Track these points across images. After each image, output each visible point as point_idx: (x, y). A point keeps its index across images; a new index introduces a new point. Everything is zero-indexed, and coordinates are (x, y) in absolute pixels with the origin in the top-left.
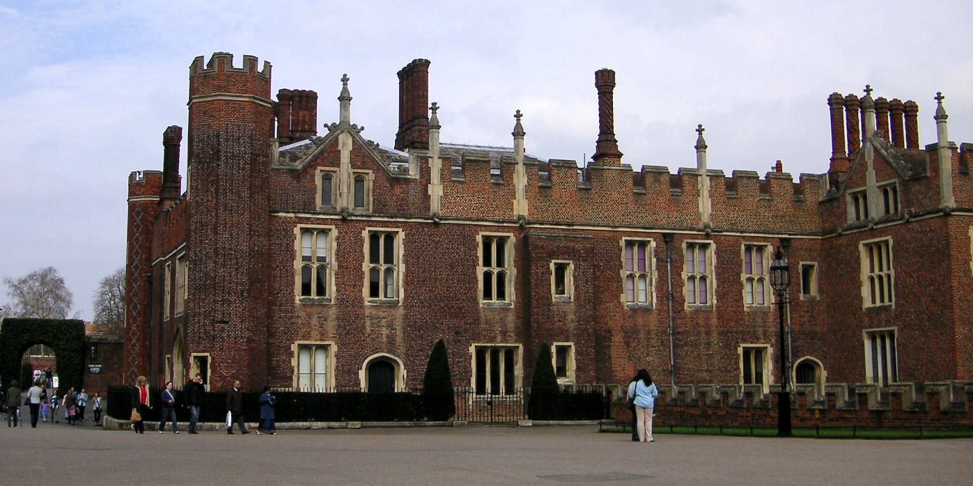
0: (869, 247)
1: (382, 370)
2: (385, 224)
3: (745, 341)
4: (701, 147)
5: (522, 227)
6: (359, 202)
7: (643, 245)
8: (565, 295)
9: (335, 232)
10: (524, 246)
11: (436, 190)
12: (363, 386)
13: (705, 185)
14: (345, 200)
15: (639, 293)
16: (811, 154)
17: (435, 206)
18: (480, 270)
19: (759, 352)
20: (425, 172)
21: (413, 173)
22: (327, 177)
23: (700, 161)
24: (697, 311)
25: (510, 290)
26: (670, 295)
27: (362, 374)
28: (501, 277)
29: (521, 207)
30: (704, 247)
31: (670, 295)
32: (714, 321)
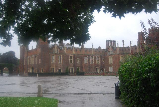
0: (110, 57)
1: (60, 70)
2: (60, 55)
3: (96, 67)
4: (92, 46)
5: (74, 54)
6: (57, 52)
7: (86, 57)
8: (79, 62)
9: (55, 56)
10: (74, 57)
11: (65, 51)
12: (58, 72)
13: (93, 50)
14: (56, 52)
15: (86, 62)
16: (104, 47)
17: (65, 53)
18: (70, 60)
19: (98, 68)
20: (64, 49)
21: (63, 49)
22: (54, 50)
23: (92, 47)
24: (92, 64)
25: (73, 62)
26: (89, 62)
27: (58, 71)
28: (72, 60)
29: (74, 53)
30: (93, 57)
31: (89, 62)
32: (93, 65)
